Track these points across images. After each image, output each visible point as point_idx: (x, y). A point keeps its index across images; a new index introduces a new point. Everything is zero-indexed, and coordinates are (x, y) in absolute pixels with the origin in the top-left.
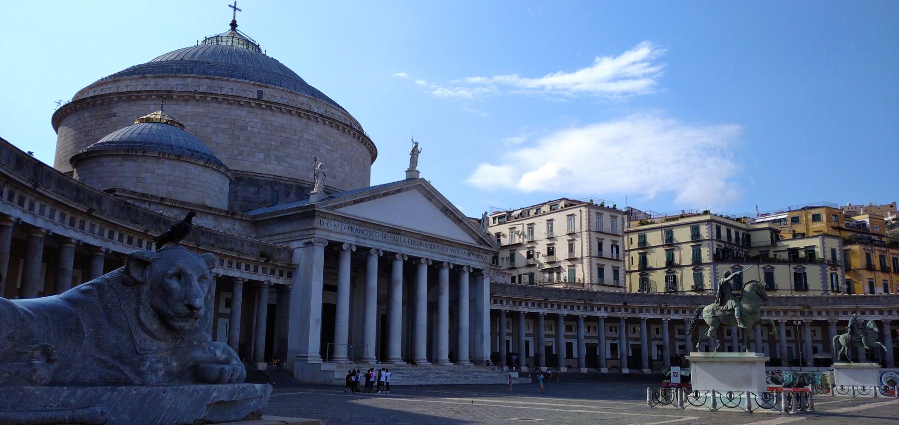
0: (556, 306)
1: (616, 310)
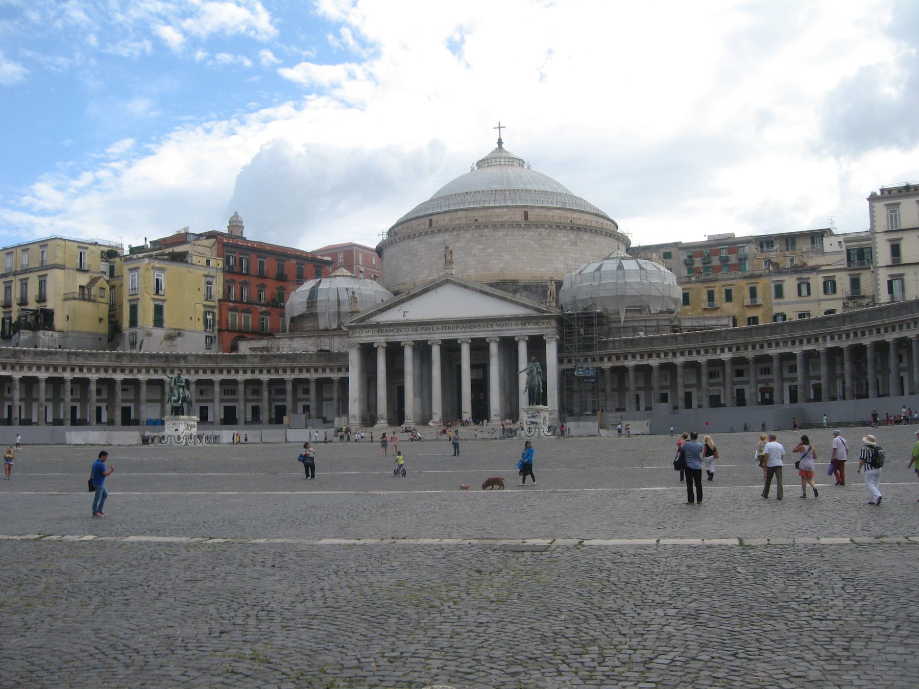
0: (670, 355)
1: (742, 348)
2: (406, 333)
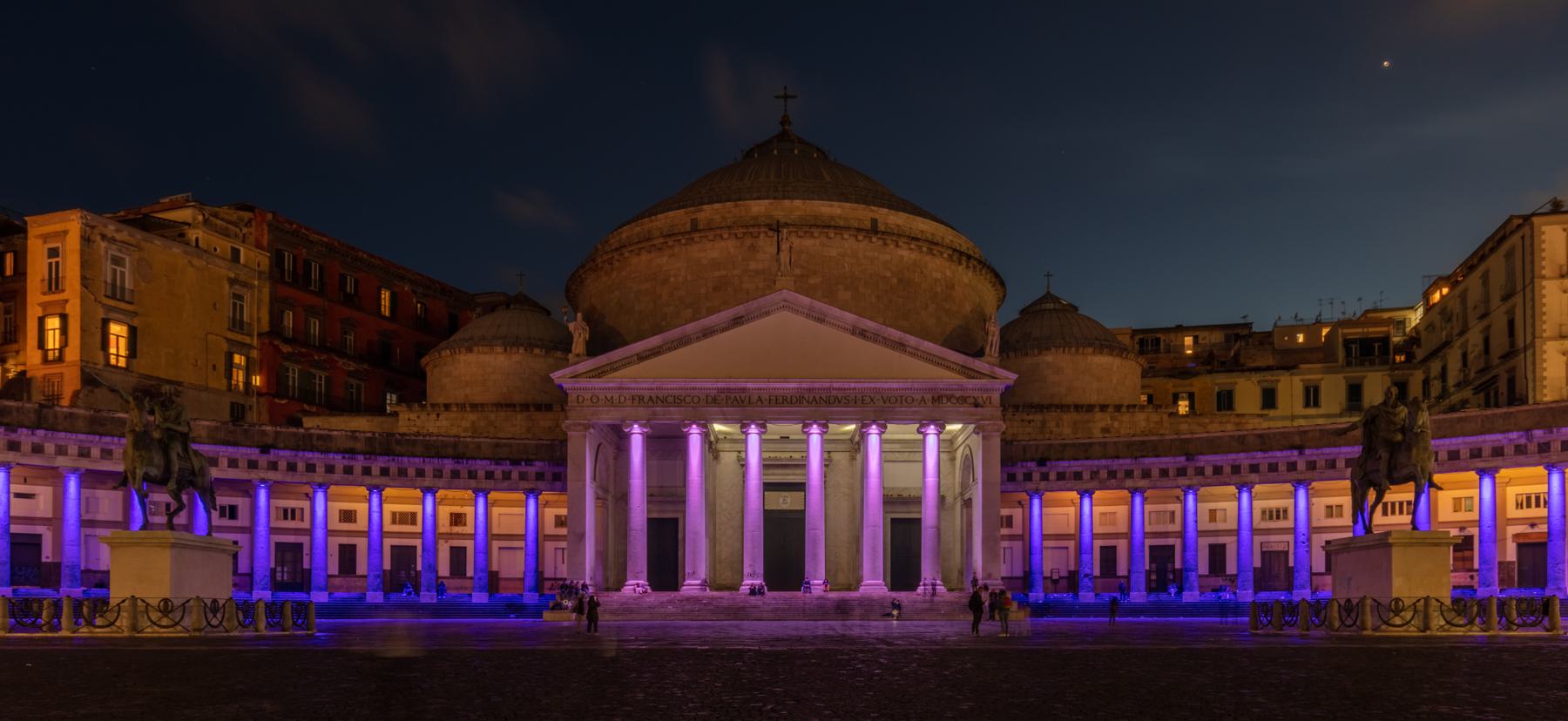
2: (692, 404)
